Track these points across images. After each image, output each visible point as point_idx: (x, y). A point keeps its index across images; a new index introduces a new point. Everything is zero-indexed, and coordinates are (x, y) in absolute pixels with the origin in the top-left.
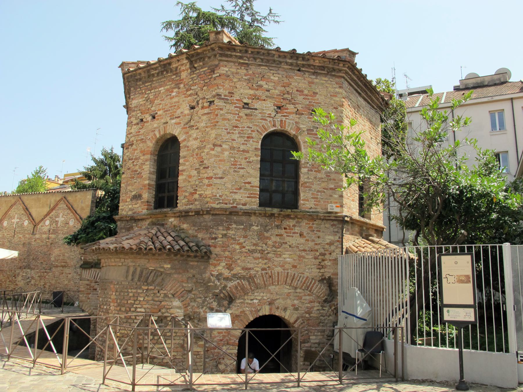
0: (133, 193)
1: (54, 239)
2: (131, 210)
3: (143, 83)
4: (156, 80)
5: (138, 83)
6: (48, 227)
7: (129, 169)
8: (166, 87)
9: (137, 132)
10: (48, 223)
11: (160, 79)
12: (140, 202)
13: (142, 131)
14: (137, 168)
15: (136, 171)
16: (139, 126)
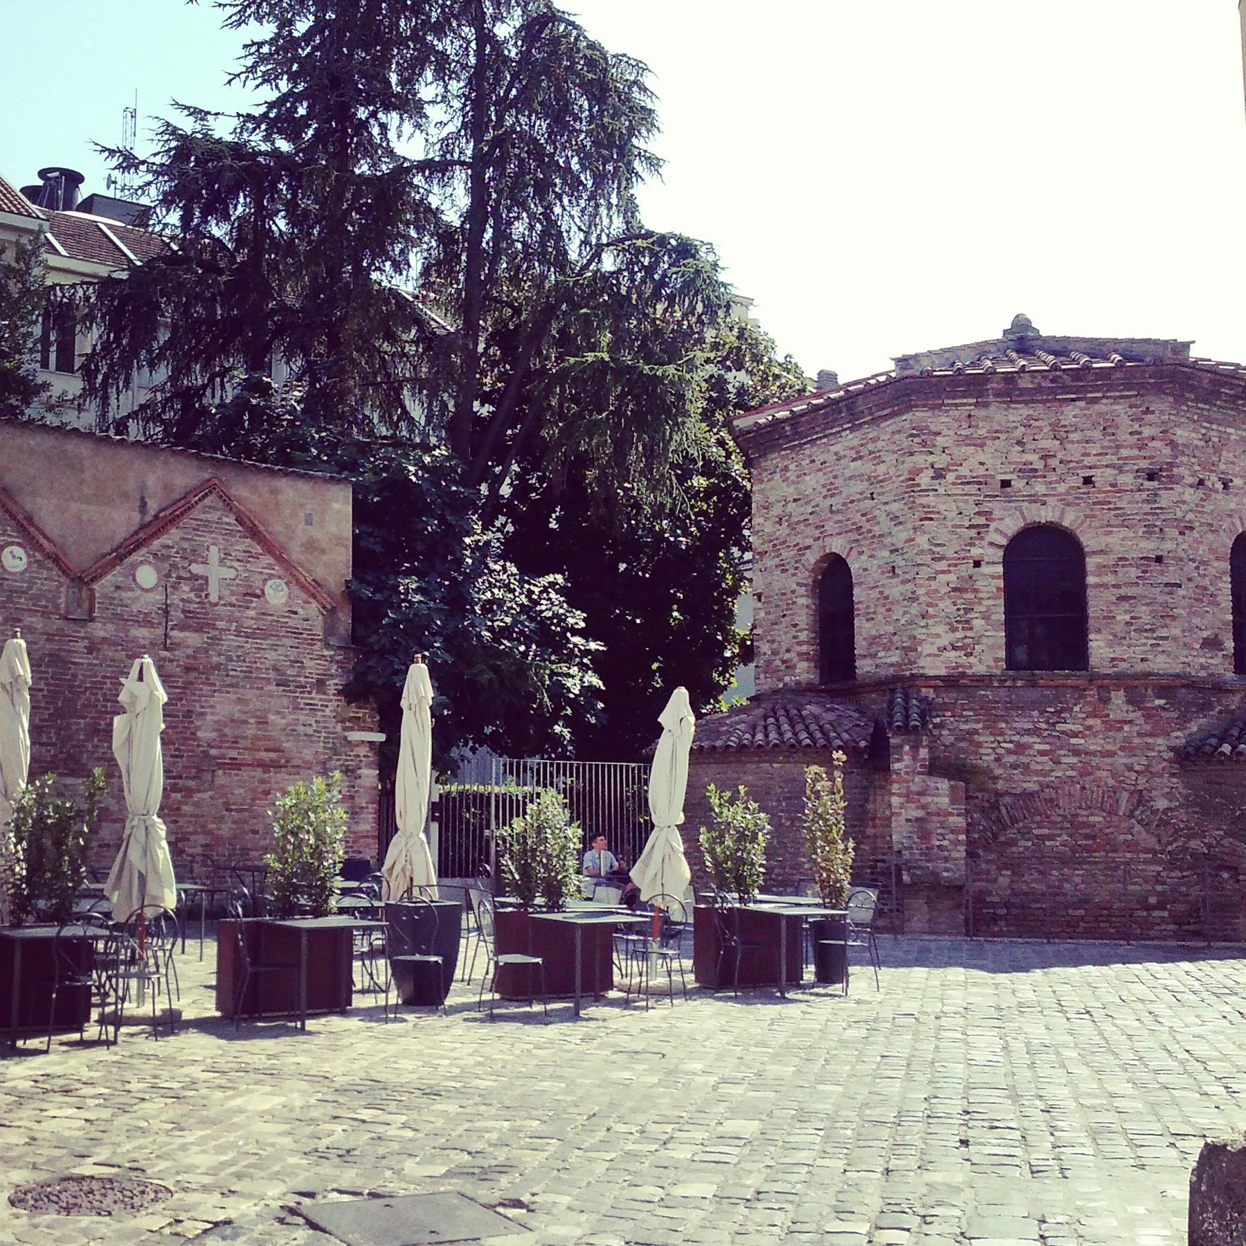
0: (1205, 634)
1: (197, 650)
2: (1203, 667)
3: (1197, 400)
4: (1220, 407)
5: (1187, 395)
6: (159, 597)
7: (1190, 580)
8: (1240, 432)
9: (1197, 505)
10: (147, 576)
11: (1227, 408)
12: (1220, 654)
13: (1209, 507)
14: (1206, 582)
15: (1205, 589)
16: (1200, 493)
